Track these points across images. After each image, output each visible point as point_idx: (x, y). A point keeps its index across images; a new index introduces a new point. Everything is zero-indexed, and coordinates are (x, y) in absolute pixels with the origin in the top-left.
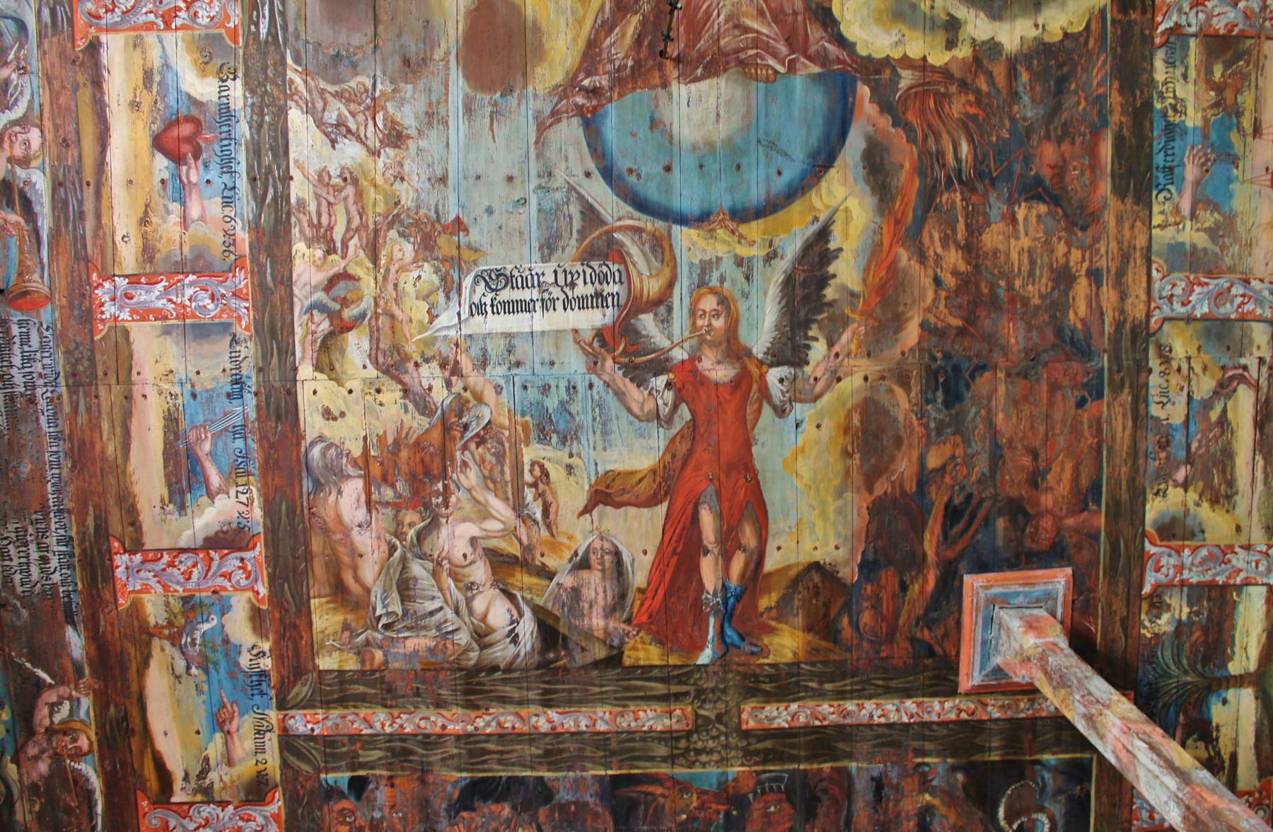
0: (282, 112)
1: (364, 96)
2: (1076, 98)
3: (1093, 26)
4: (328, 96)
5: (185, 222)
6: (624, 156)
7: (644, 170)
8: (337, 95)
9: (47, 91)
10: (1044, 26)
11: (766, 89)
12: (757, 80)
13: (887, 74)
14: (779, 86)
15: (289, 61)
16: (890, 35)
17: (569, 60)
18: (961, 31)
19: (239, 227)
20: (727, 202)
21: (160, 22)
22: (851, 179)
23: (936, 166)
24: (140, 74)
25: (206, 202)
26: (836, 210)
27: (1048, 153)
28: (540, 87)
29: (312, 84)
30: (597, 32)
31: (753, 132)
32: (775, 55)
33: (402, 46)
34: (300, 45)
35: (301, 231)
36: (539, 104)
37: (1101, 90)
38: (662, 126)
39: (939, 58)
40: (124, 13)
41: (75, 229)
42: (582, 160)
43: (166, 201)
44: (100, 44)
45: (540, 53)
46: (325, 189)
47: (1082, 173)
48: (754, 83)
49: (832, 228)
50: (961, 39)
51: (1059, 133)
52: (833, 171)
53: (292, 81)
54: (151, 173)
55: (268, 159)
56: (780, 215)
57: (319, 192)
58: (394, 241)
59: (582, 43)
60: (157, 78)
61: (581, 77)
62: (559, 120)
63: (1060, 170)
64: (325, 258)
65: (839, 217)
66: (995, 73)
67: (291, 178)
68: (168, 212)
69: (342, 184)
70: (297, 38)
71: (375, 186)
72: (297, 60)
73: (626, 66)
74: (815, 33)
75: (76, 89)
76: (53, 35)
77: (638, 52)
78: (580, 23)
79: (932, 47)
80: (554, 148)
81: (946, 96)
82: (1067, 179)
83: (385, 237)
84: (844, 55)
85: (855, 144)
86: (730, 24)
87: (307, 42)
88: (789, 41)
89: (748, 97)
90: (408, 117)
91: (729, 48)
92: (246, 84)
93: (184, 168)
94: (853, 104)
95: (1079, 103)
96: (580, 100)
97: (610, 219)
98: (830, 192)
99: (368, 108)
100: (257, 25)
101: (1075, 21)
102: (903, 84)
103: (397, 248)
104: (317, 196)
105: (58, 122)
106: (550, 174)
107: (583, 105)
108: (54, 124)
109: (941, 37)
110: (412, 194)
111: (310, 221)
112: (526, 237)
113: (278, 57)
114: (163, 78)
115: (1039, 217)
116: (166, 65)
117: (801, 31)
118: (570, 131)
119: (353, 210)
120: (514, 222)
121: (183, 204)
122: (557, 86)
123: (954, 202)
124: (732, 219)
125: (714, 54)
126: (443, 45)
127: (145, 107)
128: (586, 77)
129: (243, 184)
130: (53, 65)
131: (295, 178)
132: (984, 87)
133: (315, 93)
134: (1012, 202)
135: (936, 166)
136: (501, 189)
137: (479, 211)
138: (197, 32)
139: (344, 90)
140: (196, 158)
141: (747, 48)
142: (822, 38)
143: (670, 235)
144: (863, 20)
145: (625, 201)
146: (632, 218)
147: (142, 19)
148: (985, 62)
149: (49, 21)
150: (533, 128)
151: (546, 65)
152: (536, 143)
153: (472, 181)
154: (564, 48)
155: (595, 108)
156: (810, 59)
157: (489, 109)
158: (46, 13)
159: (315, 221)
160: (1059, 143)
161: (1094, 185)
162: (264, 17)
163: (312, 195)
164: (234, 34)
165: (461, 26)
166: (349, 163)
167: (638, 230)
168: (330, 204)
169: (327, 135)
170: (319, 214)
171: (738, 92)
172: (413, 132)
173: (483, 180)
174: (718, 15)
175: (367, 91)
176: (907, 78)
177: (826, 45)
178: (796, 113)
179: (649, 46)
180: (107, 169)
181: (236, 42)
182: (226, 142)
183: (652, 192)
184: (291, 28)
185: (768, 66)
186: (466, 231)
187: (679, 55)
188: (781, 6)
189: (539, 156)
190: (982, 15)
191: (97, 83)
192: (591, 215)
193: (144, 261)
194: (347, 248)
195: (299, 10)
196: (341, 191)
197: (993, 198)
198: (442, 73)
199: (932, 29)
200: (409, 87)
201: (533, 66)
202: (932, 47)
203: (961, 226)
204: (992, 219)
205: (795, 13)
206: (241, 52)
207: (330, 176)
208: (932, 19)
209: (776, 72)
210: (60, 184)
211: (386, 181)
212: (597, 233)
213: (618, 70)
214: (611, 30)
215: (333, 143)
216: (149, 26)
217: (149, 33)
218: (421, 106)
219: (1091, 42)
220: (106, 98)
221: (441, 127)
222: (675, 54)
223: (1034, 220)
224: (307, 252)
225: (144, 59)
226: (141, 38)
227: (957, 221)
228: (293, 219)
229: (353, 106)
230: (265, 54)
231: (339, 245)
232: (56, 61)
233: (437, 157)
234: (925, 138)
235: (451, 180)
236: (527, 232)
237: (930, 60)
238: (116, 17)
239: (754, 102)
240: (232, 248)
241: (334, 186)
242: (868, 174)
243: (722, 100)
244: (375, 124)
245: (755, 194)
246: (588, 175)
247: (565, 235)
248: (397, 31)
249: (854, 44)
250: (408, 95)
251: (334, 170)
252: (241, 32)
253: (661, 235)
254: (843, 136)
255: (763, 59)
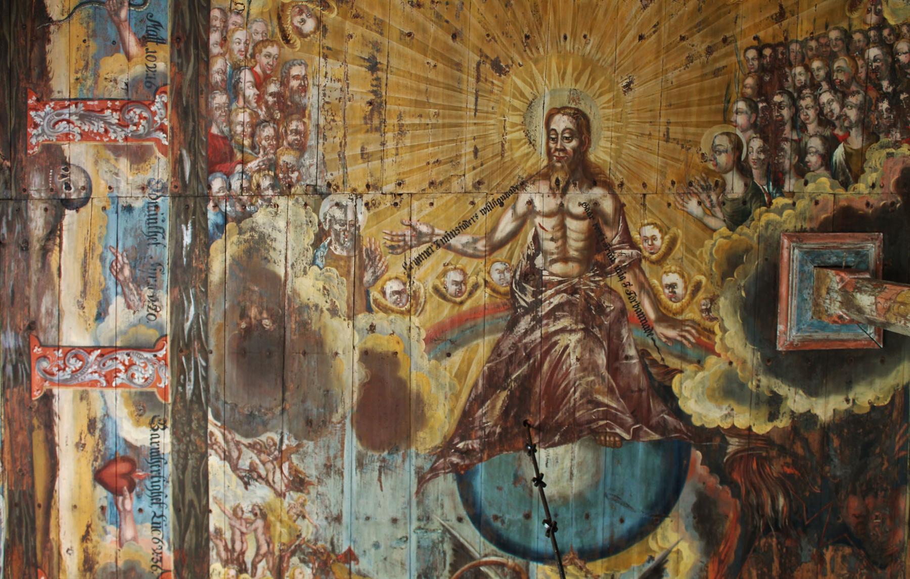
0: (204, 457)
1: (273, 448)
2: (879, 460)
3: (897, 400)
4: (242, 446)
5: (120, 542)
6: (491, 505)
7: (507, 517)
8: (251, 446)
9: (8, 430)
10: (854, 400)
11: (613, 453)
12: (606, 445)
13: (717, 441)
14: (623, 451)
15: (210, 417)
16: (721, 409)
17: (447, 428)
18: (782, 405)
19: (166, 547)
20: (576, 543)
21: (103, 380)
22: (683, 527)
23: (756, 516)
24: (85, 422)
25: (139, 527)
26: (669, 551)
27: (854, 504)
28: (421, 448)
29: (229, 437)
30: (471, 406)
31: (601, 488)
32: (622, 425)
33: (305, 410)
34: (220, 405)
35: (218, 554)
36: (420, 462)
37: (902, 454)
38: (523, 482)
39: (762, 428)
40: (73, 372)
41: (27, 540)
42: (455, 508)
43: (104, 524)
44: (53, 396)
45: (422, 420)
46: (239, 522)
47: (883, 522)
48: (603, 448)
49: (666, 566)
50: (782, 412)
51: (864, 487)
52: (668, 520)
53: (212, 434)
54: (93, 500)
55: (190, 495)
56: (622, 555)
57: (233, 523)
58: (295, 567)
59: (457, 413)
60: (99, 425)
61: (456, 441)
62: (437, 475)
63: (864, 518)
64: (237, 576)
65: (672, 557)
66: (810, 440)
67: (210, 511)
68: (106, 532)
69: (253, 517)
70: (217, 399)
71: (281, 521)
72: (217, 416)
73: (494, 432)
74: (657, 407)
75: (31, 429)
76: (15, 386)
77: (505, 421)
78: (457, 396)
79: (756, 419)
80: (432, 497)
81: (768, 459)
82: (871, 526)
83: (288, 562)
84: (681, 426)
85: (687, 498)
86: (584, 400)
87: (225, 402)
88: (633, 414)
89: (597, 460)
90: (311, 468)
91: (583, 419)
92: (174, 434)
93: (121, 499)
94: (687, 465)
95: (882, 464)
96: (455, 459)
97: (478, 555)
98: (664, 537)
99: (276, 459)
100: (184, 386)
101: (881, 396)
102: (731, 449)
103: (297, 572)
104: (232, 527)
105: (17, 455)
106: (428, 519)
107: (458, 464)
108: (12, 457)
109: (764, 411)
110: (311, 529)
111: (226, 546)
112: (407, 567)
113: (201, 413)
114: (104, 426)
115: (844, 557)
116: (107, 415)
117: (645, 405)
118: (446, 484)
119: (262, 539)
120: (397, 555)
121: (119, 527)
122: (437, 447)
123: (770, 545)
124: (580, 558)
125: (570, 424)
126: (340, 410)
127: (89, 447)
128: (461, 441)
129: (169, 512)
130: (13, 410)
131: (214, 512)
132: (800, 451)
133: (232, 444)
134: (821, 545)
135: (756, 516)
136: (387, 529)
137: (368, 545)
138: (133, 390)
139: (256, 443)
140: (131, 491)
141: (599, 419)
142: (662, 411)
143: (527, 569)
144: (698, 396)
145: (491, 541)
146: (496, 555)
147: (88, 377)
148: (802, 431)
149: (11, 375)
150: (414, 481)
151: (427, 430)
152: (417, 493)
153: (362, 521)
154: (443, 417)
155: (467, 466)
156: (651, 428)
157: (378, 464)
158: (9, 368)
159: (230, 546)
160: (864, 497)
161: (894, 531)
162: (190, 380)
163: (228, 527)
164: (164, 392)
165: (355, 396)
166: (259, 501)
167: (501, 565)
168: (242, 534)
169: (241, 478)
170: (233, 542)
171: (590, 456)
172: (314, 480)
173: (371, 521)
174: (575, 392)
175: (275, 444)
176: (734, 445)
177: (666, 416)
178: (638, 472)
179: (514, 416)
180: (56, 495)
181: (166, 399)
182: (156, 479)
183: (514, 535)
184: (212, 389)
185: (617, 434)
186: (356, 559)
187: (540, 425)
188: (629, 384)
189: (419, 503)
190: (801, 392)
191: (49, 425)
192: (461, 552)
193: (85, 570)
194: (256, 568)
195: (219, 376)
196: (252, 524)
197: (804, 542)
198: (339, 433)
199: (757, 404)
200: (311, 444)
201: (416, 431)
202: (756, 419)
203: (776, 565)
204: (803, 560)
205: (640, 390)
206: (170, 408)
207: (243, 511)
208: (758, 396)
209: (622, 439)
210: (16, 505)
211: (290, 518)
212: (466, 566)
213: (488, 436)
214: (483, 403)
215: (247, 484)
216: (93, 384)
217: (94, 389)
218: (321, 459)
219: (895, 414)
220: (57, 438)
221: (337, 477)
222: (537, 423)
223: (839, 560)
224: (223, 570)
225: (89, 410)
226: (87, 392)
227: (773, 560)
228: (211, 544)
229: (263, 456)
230: (190, 411)
231: (249, 566)
232: (16, 407)
233: (333, 501)
234: (748, 493)
235: (345, 519)
236: (407, 563)
237: (755, 429)
238: (67, 375)
239: (602, 463)
240: (159, 564)
241: (246, 520)
242: (697, 523)
243: (575, 462)
244: (282, 472)
245: (600, 536)
246: (460, 520)
247: (440, 567)
248: (301, 398)
249: (690, 416)
250: (310, 450)
251: (246, 506)
252: (170, 391)
253: (521, 569)
254: (677, 492)
255: (611, 428)
